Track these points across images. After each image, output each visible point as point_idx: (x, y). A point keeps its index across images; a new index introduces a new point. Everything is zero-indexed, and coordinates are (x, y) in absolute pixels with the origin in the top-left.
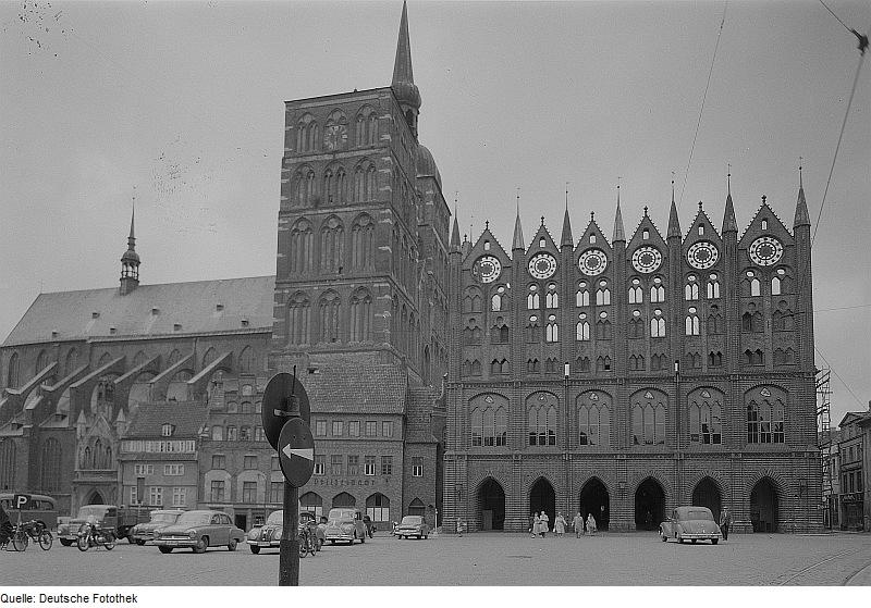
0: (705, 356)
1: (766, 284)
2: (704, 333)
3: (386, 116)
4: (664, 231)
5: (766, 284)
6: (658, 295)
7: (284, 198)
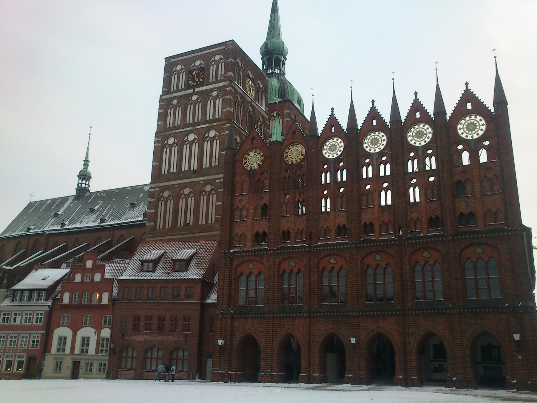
0: (424, 220)
1: (474, 157)
2: (423, 200)
3: (230, 60)
4: (387, 117)
5: (474, 157)
6: (385, 170)
7: (160, 123)
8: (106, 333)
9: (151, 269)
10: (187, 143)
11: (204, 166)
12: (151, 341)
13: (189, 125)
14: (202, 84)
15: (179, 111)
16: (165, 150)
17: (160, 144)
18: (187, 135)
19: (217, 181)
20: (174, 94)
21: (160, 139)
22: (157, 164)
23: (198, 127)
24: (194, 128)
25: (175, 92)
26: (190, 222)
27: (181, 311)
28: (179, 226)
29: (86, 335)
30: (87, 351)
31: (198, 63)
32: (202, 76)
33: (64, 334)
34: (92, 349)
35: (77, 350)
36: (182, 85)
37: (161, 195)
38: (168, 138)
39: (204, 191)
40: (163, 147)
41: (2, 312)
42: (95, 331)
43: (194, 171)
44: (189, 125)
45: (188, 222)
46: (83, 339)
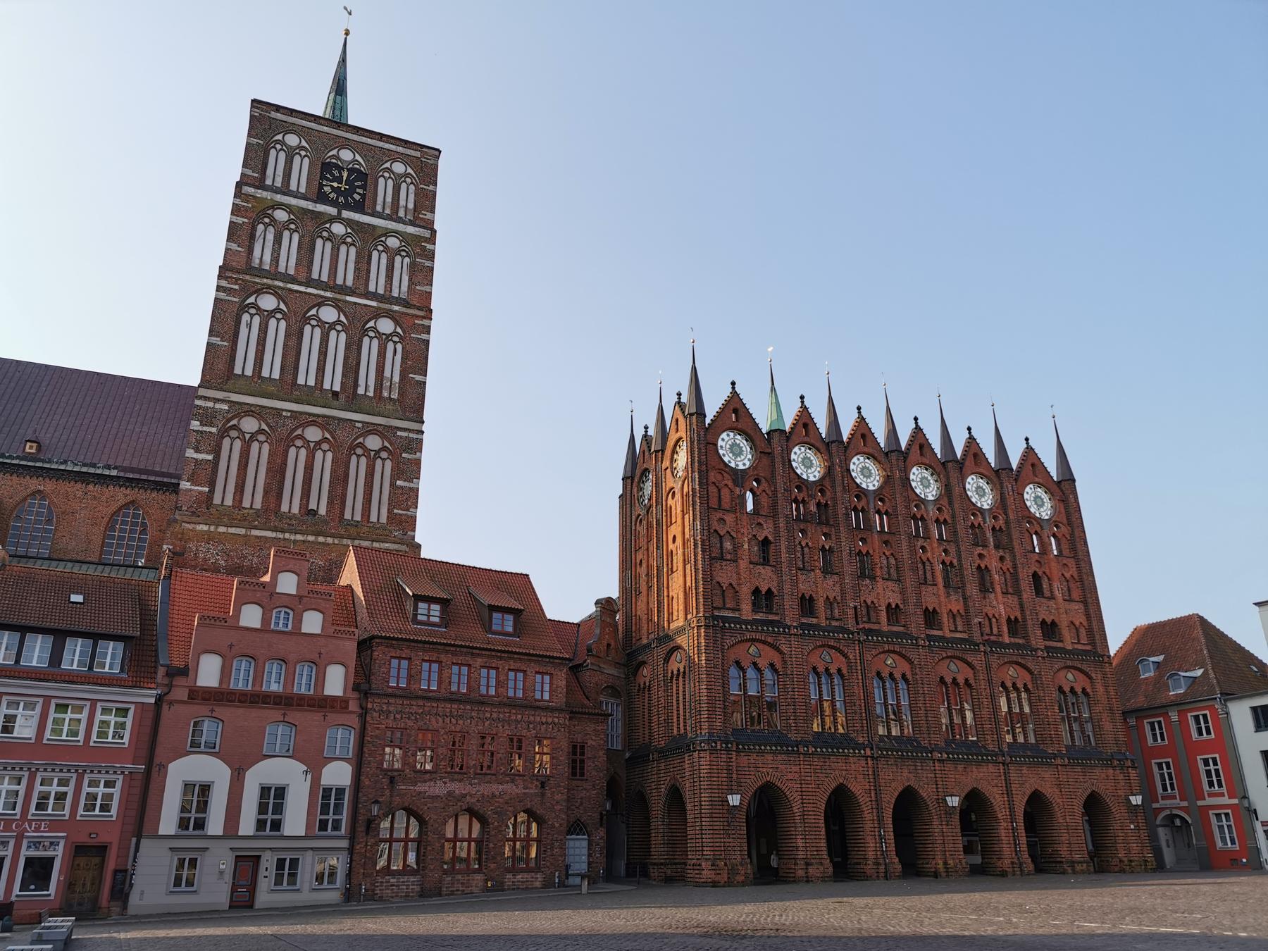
8: (338, 774)
9: (437, 620)
11: (361, 391)
12: (464, 796)
14: (359, 207)
15: (291, 243)
16: (246, 317)
17: (237, 300)
18: (319, 305)
19: (399, 433)
20: (279, 196)
21: (236, 287)
22: (225, 344)
23: (348, 298)
24: (338, 296)
25: (273, 189)
26: (318, 508)
27: (531, 726)
28: (287, 511)
29: (274, 780)
30: (277, 825)
31: (346, 155)
32: (360, 191)
33: (200, 777)
34: (295, 820)
35: (247, 825)
37: (231, 423)
38: (259, 292)
39: (362, 445)
40: (244, 308)
41: (4, 698)
42: (306, 768)
43: (335, 394)
45: (313, 506)
46: (265, 791)
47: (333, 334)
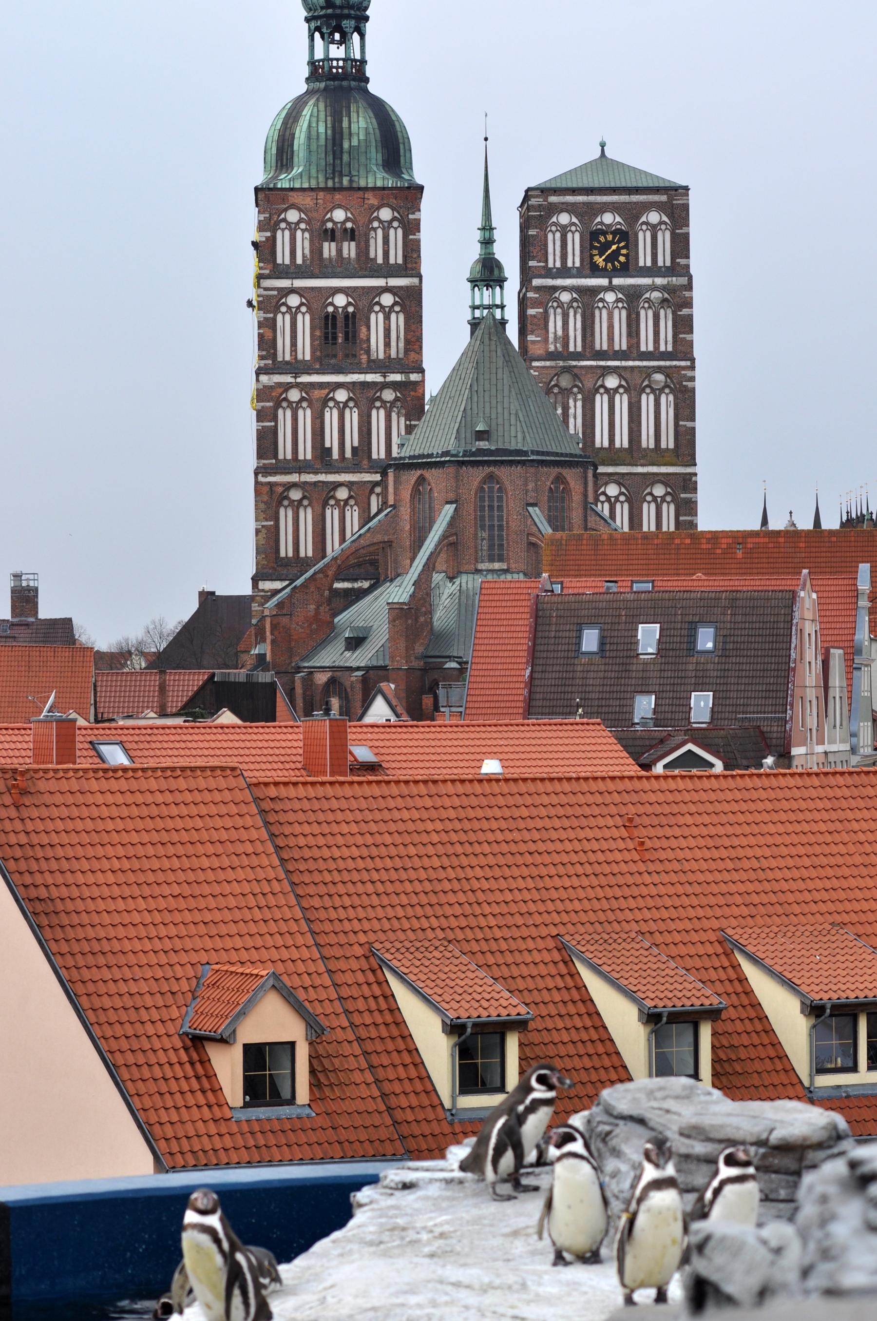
10: (602, 390)
13: (601, 355)
14: (625, 270)
18: (603, 376)
32: (624, 251)
36: (574, 260)
44: (601, 355)
47: (617, 398)
